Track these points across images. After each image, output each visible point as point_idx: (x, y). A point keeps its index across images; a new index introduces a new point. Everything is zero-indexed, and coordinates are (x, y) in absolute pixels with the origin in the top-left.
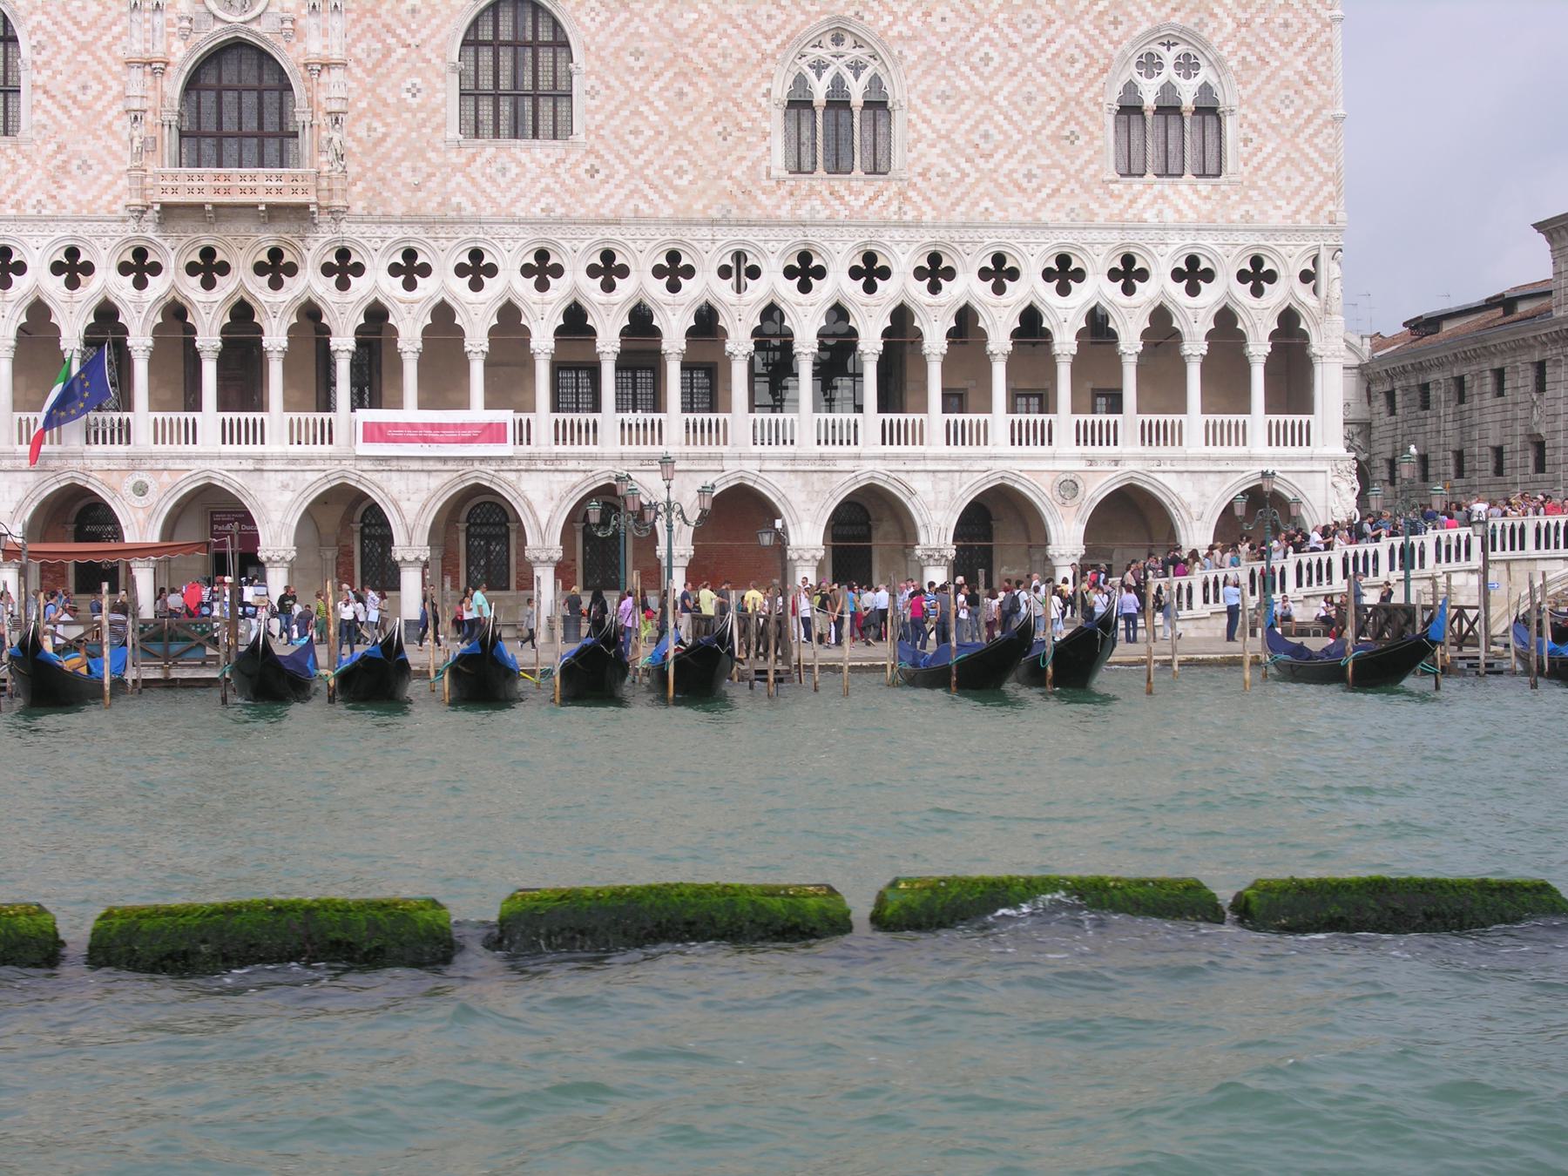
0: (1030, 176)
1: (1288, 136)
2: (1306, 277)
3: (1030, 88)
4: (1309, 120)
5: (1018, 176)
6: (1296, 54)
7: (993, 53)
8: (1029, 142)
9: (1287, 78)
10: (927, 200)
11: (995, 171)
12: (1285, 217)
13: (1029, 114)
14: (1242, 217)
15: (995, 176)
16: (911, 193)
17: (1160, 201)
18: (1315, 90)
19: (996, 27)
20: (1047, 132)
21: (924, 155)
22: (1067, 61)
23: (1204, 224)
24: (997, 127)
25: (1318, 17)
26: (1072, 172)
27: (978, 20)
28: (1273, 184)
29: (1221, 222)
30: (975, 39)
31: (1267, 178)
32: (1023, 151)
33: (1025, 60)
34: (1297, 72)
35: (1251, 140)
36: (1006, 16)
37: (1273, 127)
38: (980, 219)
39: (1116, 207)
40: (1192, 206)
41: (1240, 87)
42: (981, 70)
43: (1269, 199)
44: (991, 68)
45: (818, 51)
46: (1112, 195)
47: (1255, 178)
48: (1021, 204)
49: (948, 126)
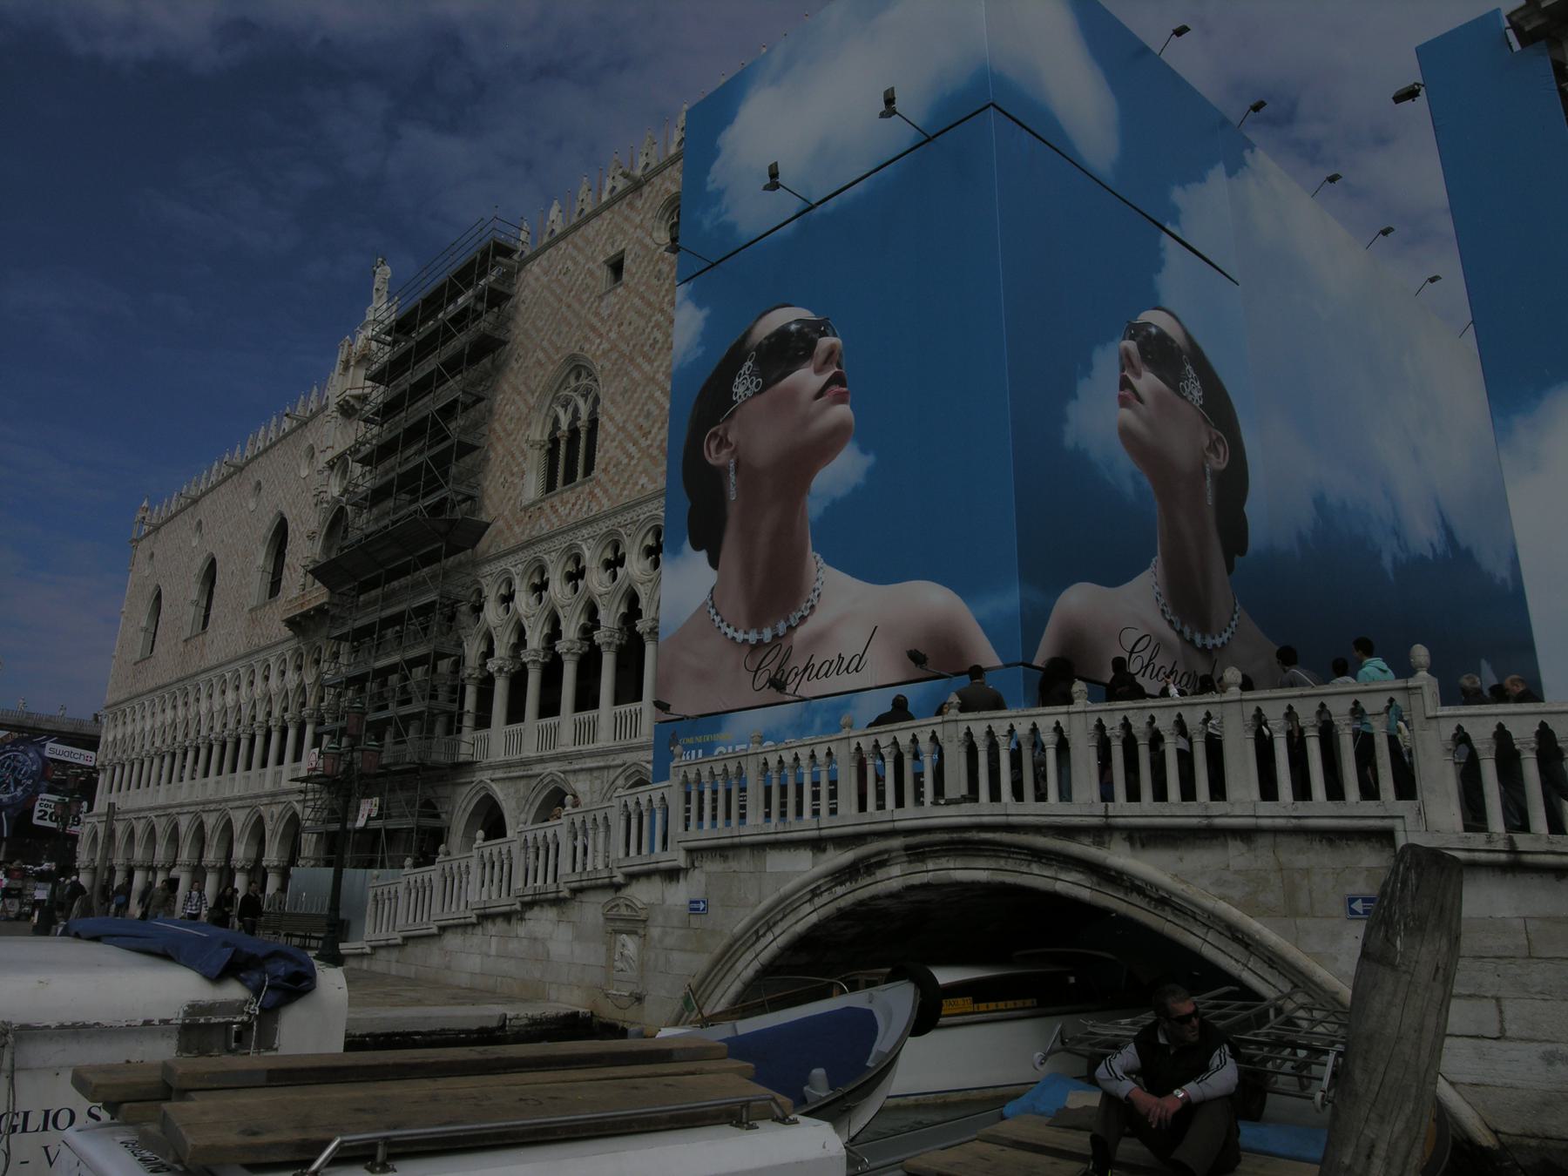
10: (606, 491)
16: (597, 490)
21: (607, 452)
45: (566, 393)
49: (625, 417)
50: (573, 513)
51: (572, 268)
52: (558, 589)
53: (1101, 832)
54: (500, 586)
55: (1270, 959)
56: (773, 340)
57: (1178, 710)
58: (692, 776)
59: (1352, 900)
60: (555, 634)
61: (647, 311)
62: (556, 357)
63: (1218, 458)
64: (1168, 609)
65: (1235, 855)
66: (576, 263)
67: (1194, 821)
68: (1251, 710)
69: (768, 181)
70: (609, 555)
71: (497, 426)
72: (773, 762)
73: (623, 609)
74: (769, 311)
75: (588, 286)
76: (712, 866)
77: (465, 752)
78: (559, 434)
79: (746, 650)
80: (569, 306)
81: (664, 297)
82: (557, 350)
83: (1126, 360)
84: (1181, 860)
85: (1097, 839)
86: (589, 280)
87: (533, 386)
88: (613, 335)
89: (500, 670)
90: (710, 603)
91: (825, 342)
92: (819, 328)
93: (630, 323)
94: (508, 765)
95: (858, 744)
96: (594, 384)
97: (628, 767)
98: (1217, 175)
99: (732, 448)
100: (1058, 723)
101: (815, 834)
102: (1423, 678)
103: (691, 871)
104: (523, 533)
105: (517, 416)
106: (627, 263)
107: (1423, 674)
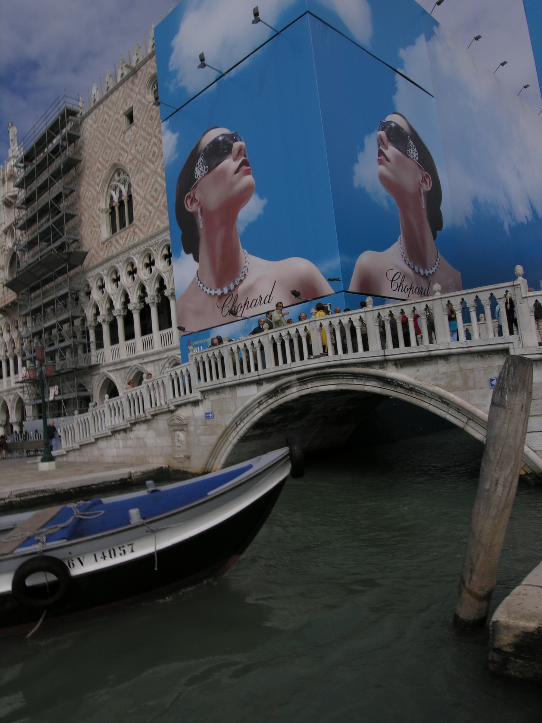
10: (141, 230)
16: (137, 230)
21: (138, 211)
30: (150, 147)
38: (155, 231)
49: (145, 193)
50: (127, 243)
51: (108, 118)
52: (125, 280)
53: (383, 363)
54: (97, 282)
55: (458, 409)
56: (211, 146)
57: (414, 305)
58: (199, 359)
59: (492, 380)
60: (127, 301)
61: (148, 137)
62: (107, 166)
63: (427, 184)
64: (407, 259)
65: (442, 367)
66: (109, 116)
67: (423, 354)
68: (445, 302)
69: (199, 63)
70: (147, 261)
71: (83, 203)
72: (235, 348)
73: (157, 286)
74: (208, 131)
75: (117, 127)
76: (213, 397)
77: (94, 361)
78: (114, 204)
79: (216, 299)
80: (109, 139)
81: (156, 129)
82: (107, 162)
83: (381, 142)
84: (418, 371)
85: (382, 366)
86: (117, 124)
87: (97, 181)
88: (133, 151)
89: (104, 321)
90: (197, 278)
91: (237, 145)
92: (234, 138)
93: (141, 145)
94: (115, 364)
95: (272, 336)
96: (128, 178)
97: (170, 358)
98: (421, 41)
99: (198, 202)
100: (360, 317)
101: (257, 378)
102: (521, 280)
103: (204, 401)
104: (104, 254)
105: (92, 197)
106: (135, 113)
107: (520, 278)
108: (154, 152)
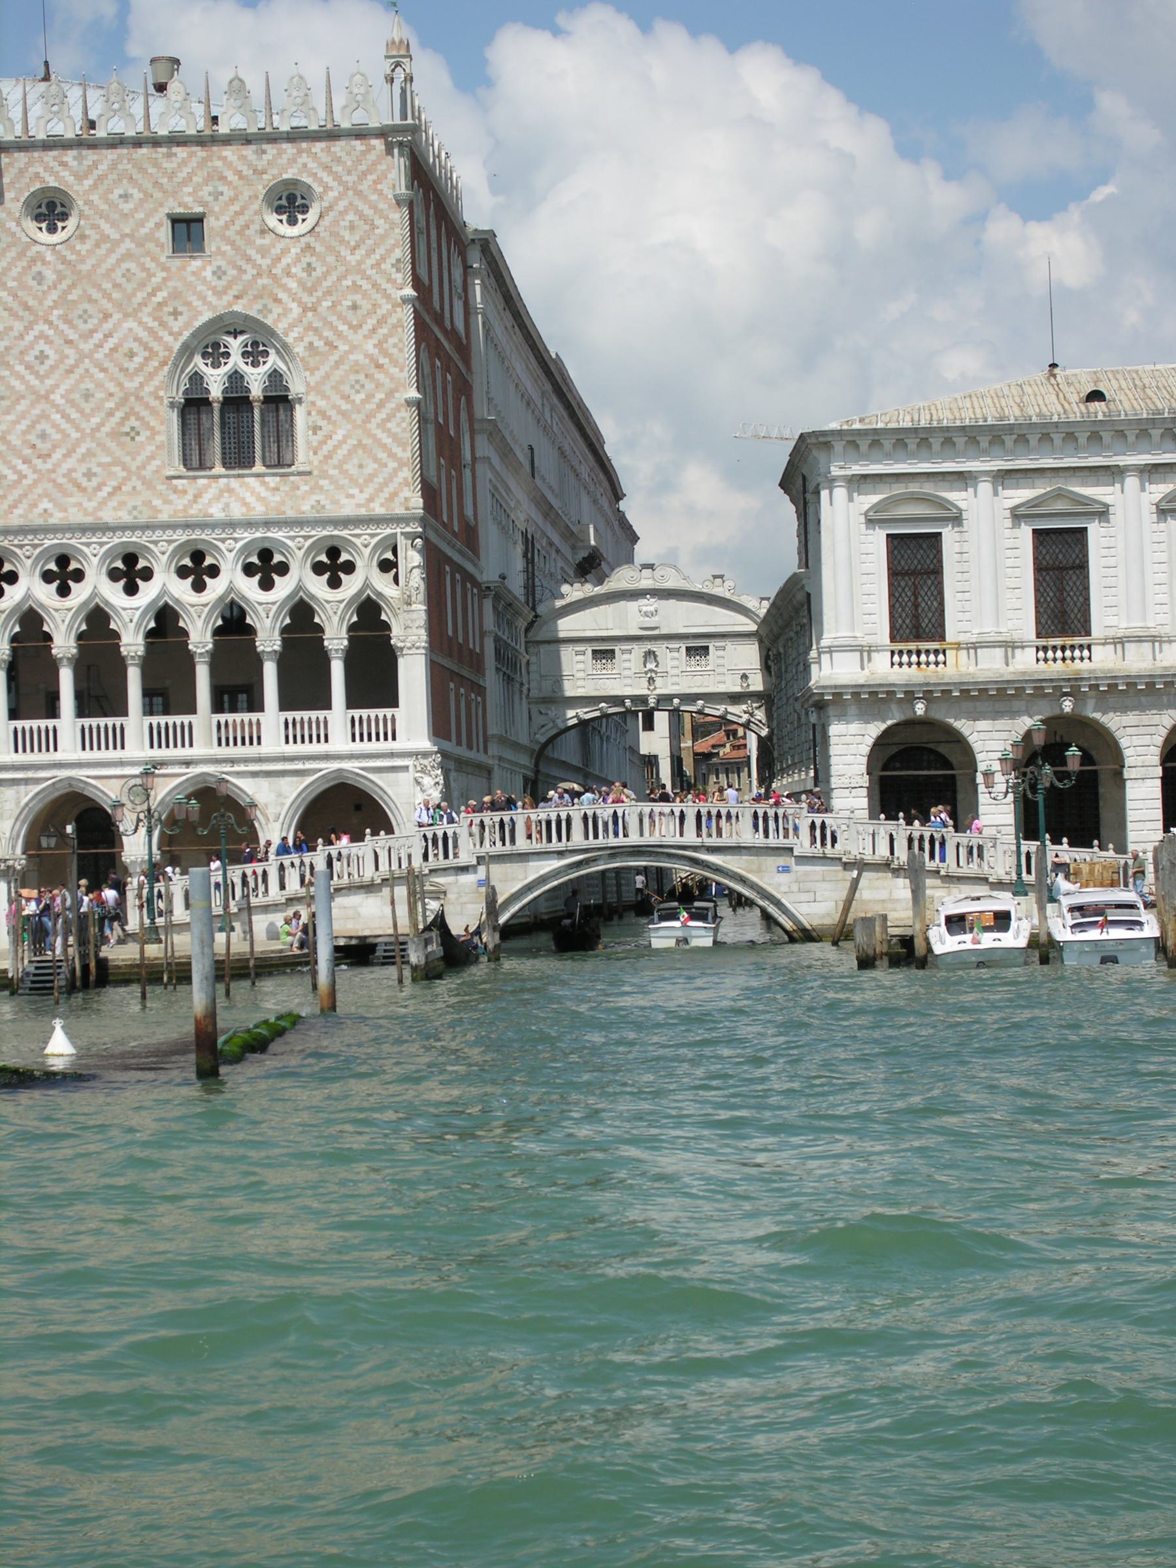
0: (89, 475)
1: (359, 422)
2: (386, 566)
3: (88, 385)
4: (381, 405)
5: (78, 476)
6: (365, 337)
7: (49, 351)
8: (88, 439)
9: (356, 361)
11: (54, 471)
12: (359, 506)
13: (88, 411)
14: (313, 507)
15: (53, 476)
17: (226, 494)
18: (387, 373)
19: (50, 323)
20: (106, 429)
22: (125, 355)
23: (273, 515)
24: (55, 426)
25: (388, 297)
26: (134, 469)
27: (32, 318)
28: (345, 473)
29: (291, 514)
30: (29, 338)
31: (339, 467)
32: (82, 450)
33: (82, 356)
34: (367, 355)
35: (320, 428)
36: (61, 312)
37: (344, 414)
38: (39, 521)
39: (180, 503)
40: (260, 498)
41: (308, 374)
42: (36, 368)
43: (339, 487)
44: (46, 367)
46: (175, 491)
47: (325, 467)
48: (80, 504)
81: (52, 308)
108: (42, 357)
